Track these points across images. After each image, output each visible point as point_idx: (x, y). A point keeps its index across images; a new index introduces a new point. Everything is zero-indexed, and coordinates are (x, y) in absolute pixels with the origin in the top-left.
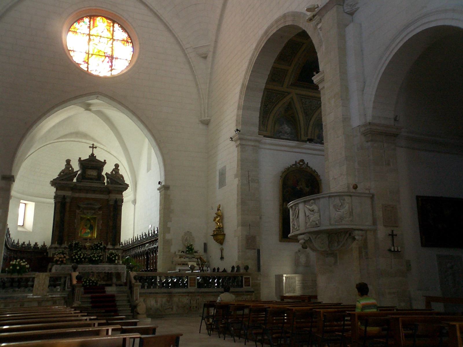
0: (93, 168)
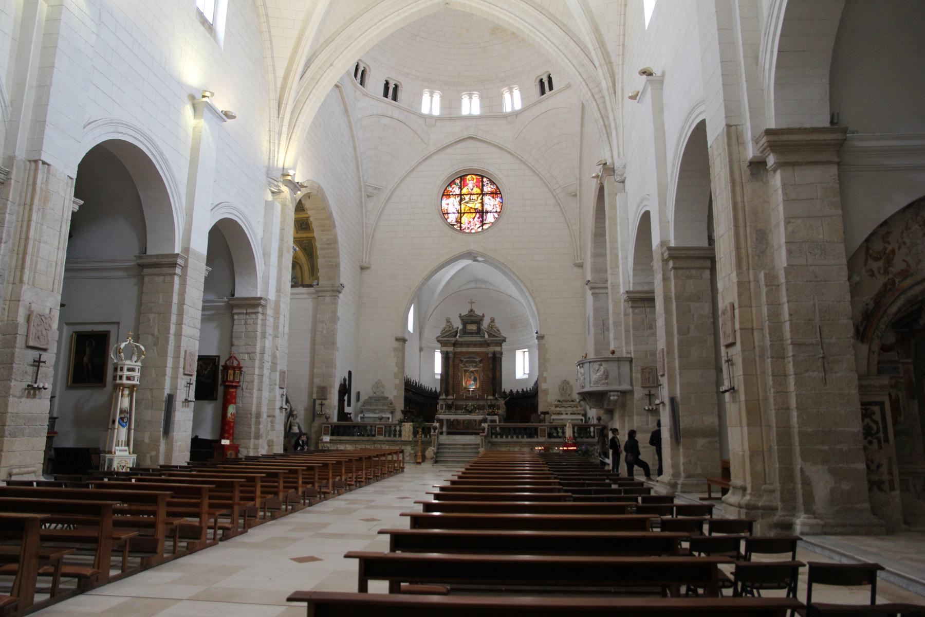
0: (473, 323)
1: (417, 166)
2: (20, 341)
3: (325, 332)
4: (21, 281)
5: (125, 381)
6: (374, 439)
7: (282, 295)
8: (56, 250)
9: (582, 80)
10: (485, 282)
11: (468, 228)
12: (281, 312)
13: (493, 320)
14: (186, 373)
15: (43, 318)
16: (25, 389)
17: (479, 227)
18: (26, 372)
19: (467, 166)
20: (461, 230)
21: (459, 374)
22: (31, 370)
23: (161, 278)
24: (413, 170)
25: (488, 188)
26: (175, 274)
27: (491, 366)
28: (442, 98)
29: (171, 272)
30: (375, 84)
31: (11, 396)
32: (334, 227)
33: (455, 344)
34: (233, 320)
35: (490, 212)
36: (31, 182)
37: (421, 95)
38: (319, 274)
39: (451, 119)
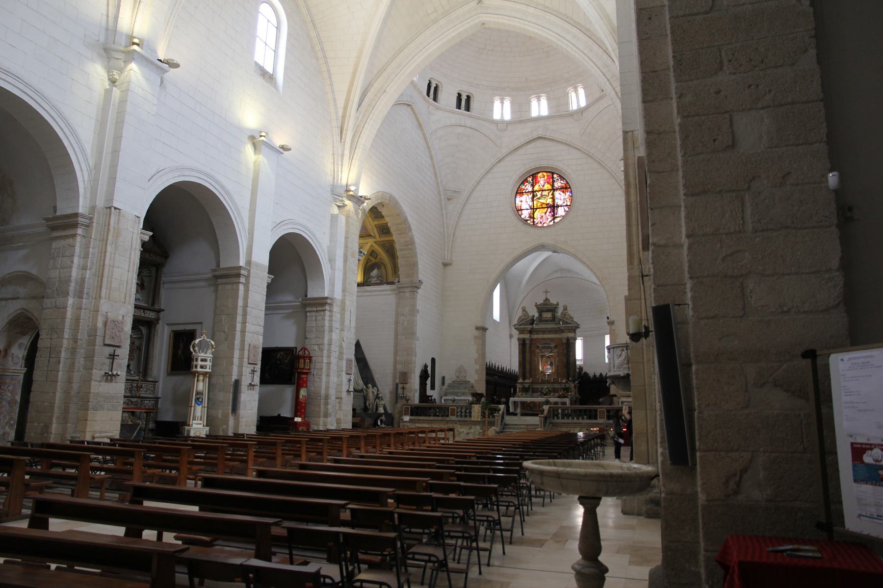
0: (548, 311)
1: (491, 169)
2: (99, 340)
3: (405, 324)
4: (100, 297)
5: (199, 369)
6: (448, 419)
7: (347, 294)
8: (127, 272)
9: (606, 80)
10: (569, 271)
11: (541, 223)
12: (346, 309)
13: (565, 308)
14: (250, 362)
15: (116, 323)
16: (104, 376)
17: (551, 221)
18: (104, 363)
19: (538, 164)
20: (534, 224)
21: (536, 359)
22: (108, 361)
23: (229, 287)
24: (488, 172)
25: (558, 184)
26: (239, 283)
27: (565, 351)
28: (512, 103)
29: (237, 281)
30: (448, 98)
31: (93, 381)
32: (410, 229)
33: (531, 332)
34: (307, 317)
35: (561, 206)
36: (107, 224)
37: (492, 103)
38: (399, 273)
39: (521, 122)
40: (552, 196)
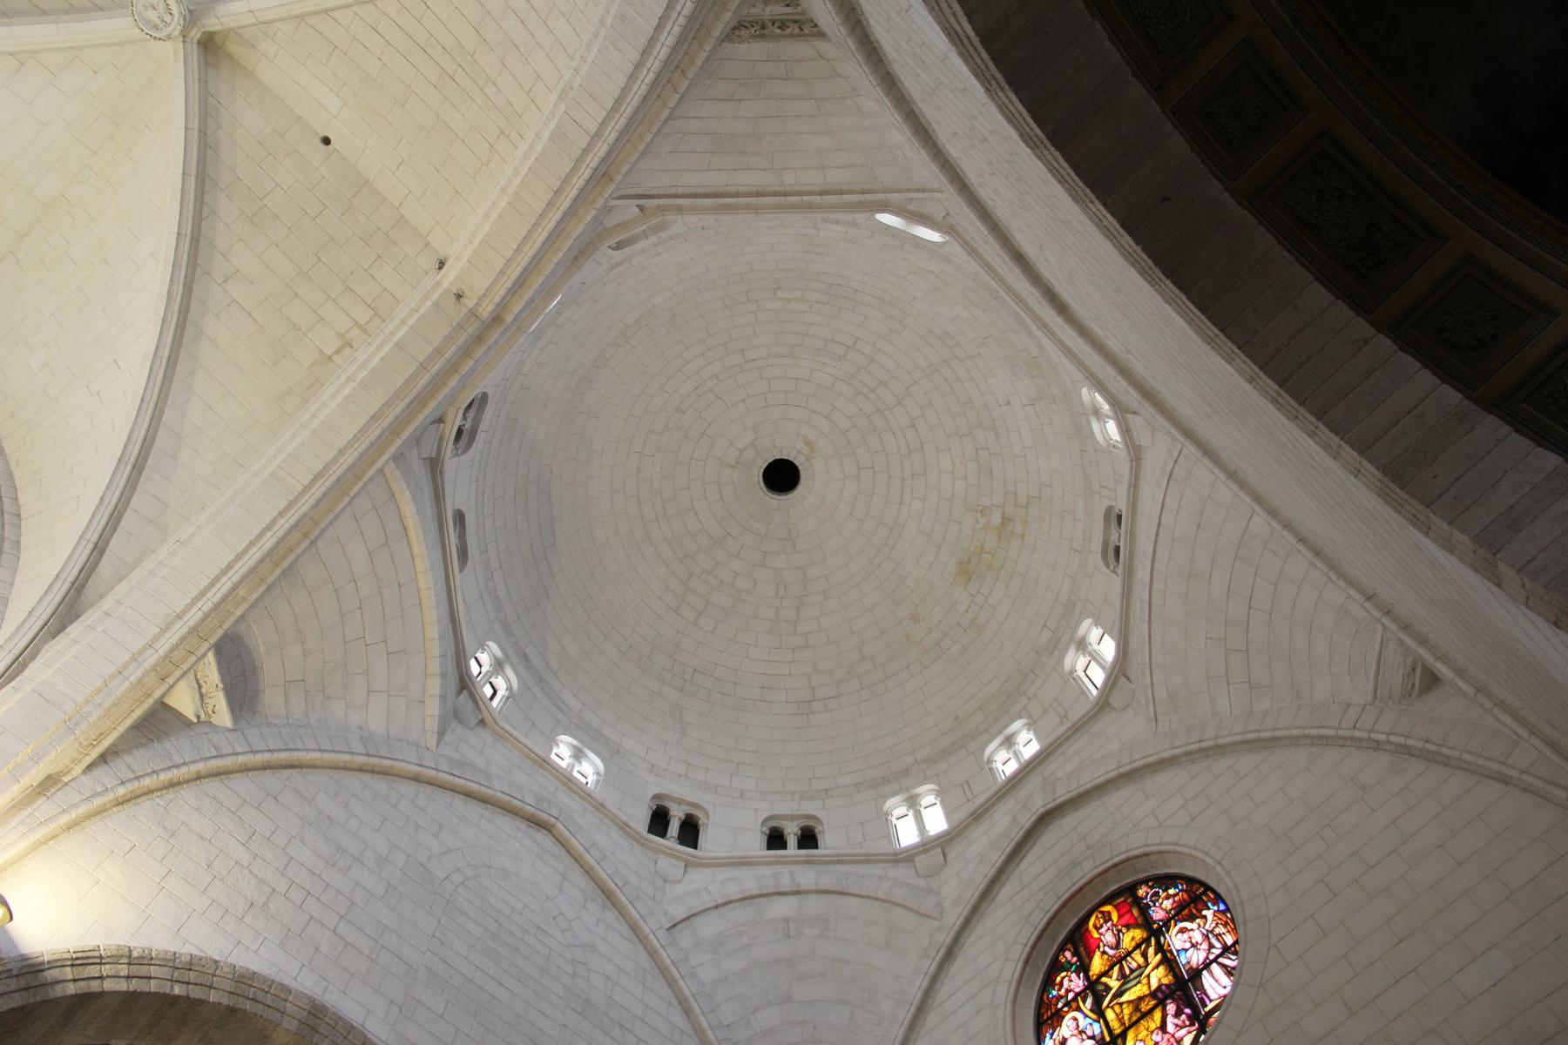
35: (1207, 965)
40: (1159, 956)
